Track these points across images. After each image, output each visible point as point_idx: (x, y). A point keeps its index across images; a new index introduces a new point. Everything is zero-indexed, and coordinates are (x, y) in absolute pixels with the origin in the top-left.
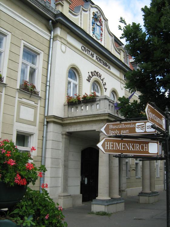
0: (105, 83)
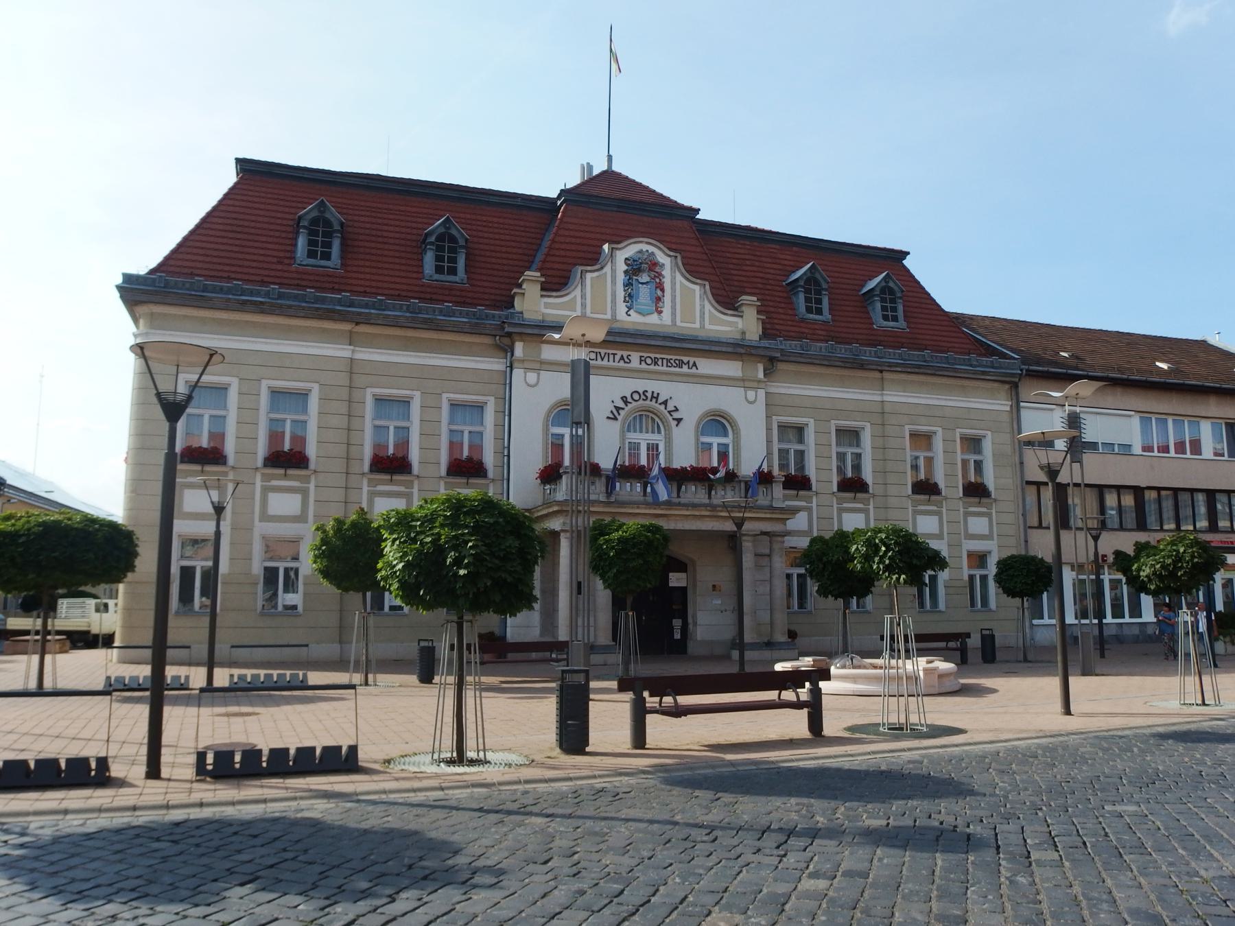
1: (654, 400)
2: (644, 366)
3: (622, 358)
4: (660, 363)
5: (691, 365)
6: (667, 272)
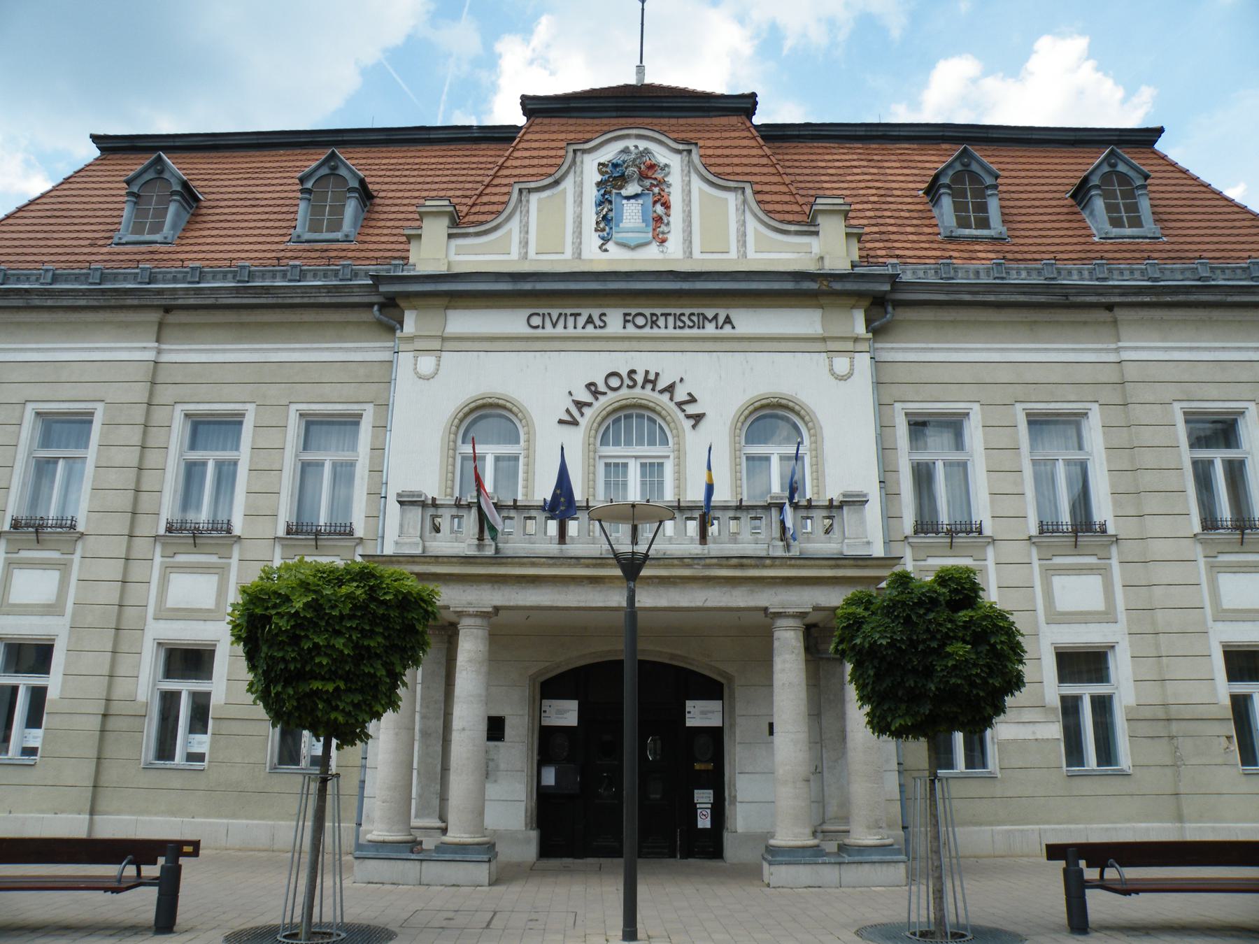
0: (690, 394)
1: (649, 386)
2: (631, 329)
3: (590, 320)
4: (661, 322)
5: (721, 320)
6: (675, 179)
